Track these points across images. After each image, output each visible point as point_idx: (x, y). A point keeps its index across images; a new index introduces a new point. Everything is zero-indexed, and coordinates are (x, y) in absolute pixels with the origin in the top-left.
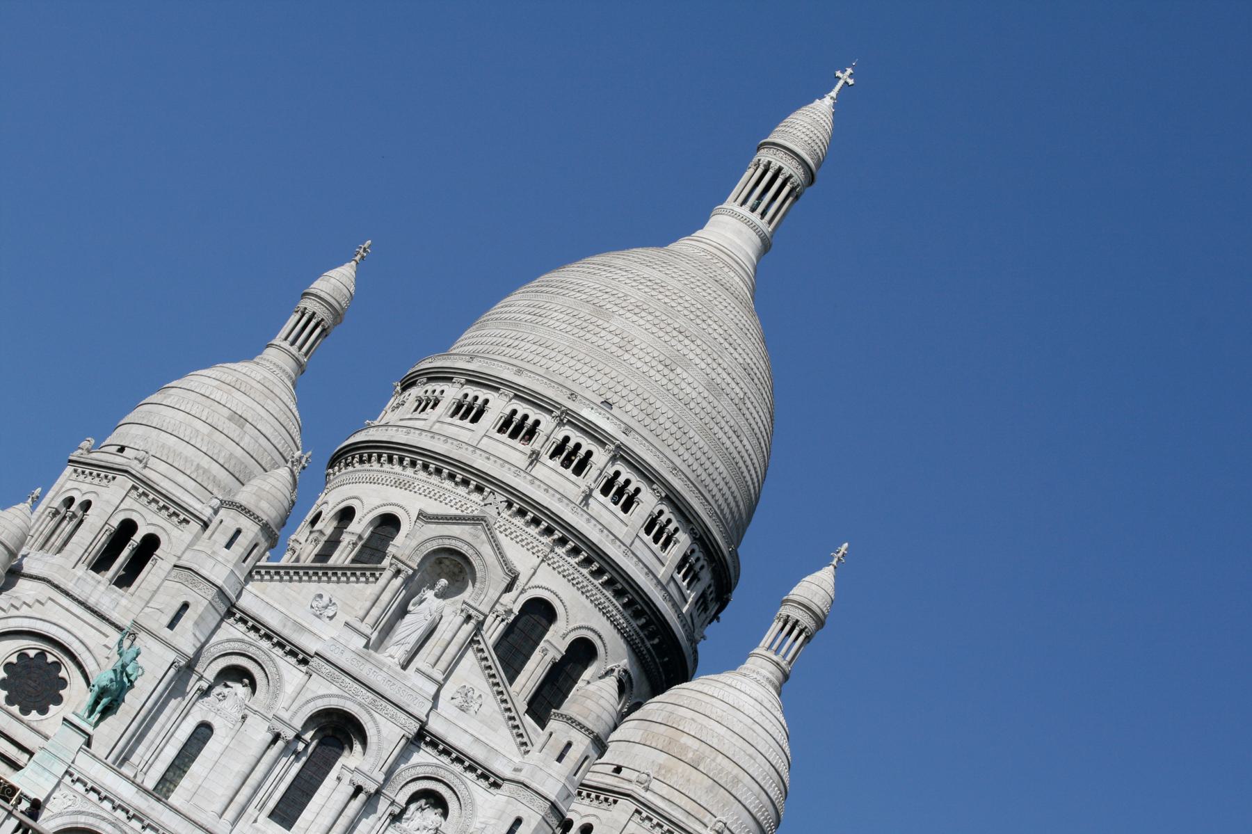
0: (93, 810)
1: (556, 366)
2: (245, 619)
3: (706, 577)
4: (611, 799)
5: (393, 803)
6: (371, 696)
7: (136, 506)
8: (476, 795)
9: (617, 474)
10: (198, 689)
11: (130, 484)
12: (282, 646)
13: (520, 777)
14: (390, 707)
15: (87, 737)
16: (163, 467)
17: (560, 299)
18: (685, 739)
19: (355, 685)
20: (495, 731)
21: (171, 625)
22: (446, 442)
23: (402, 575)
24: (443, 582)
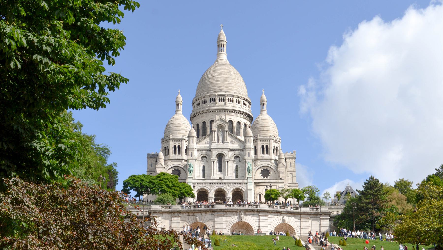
5: (232, 160)
7: (174, 143)
9: (228, 98)
16: (174, 136)
17: (206, 80)
22: (204, 108)
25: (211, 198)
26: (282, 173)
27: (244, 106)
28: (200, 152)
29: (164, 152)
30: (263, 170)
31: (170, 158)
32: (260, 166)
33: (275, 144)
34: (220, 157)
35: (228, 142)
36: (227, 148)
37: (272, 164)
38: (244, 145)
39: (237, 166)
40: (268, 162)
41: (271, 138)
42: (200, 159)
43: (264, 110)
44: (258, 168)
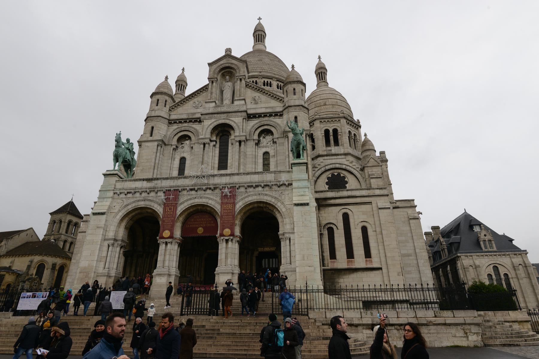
0: (132, 200)
2: (175, 122)
4: (312, 124)
5: (254, 140)
6: (225, 115)
8: (277, 122)
9: (264, 81)
10: (173, 149)
13: (287, 105)
14: (233, 114)
15: (116, 176)
18: (318, 102)
19: (219, 115)
20: (270, 103)
21: (151, 136)
23: (214, 82)
24: (227, 77)
26: (377, 178)
28: (175, 127)
30: (330, 176)
32: (323, 169)
33: (351, 128)
35: (244, 100)
36: (240, 110)
37: (350, 163)
38: (282, 105)
39: (266, 154)
41: (341, 115)
42: (174, 142)
43: (324, 82)
44: (320, 172)
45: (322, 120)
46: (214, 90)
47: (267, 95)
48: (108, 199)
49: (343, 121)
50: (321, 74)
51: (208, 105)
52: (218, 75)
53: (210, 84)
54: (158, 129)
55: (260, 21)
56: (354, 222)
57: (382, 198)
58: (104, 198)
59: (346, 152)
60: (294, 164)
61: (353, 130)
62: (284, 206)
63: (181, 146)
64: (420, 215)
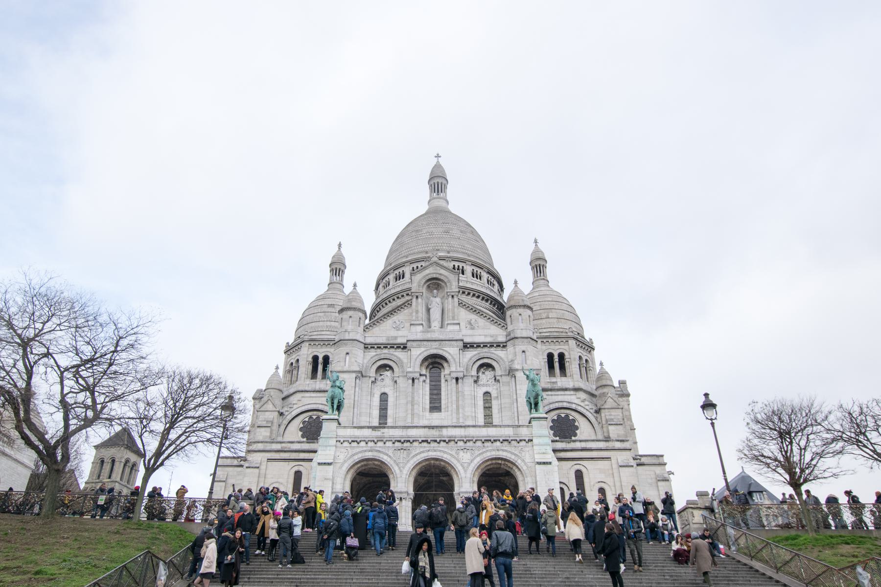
0: (358, 450)
1: (416, 250)
3: (496, 283)
7: (314, 350)
8: (500, 355)
9: (454, 266)
11: (307, 344)
12: (393, 347)
13: (512, 336)
14: (447, 342)
16: (315, 333)
19: (429, 343)
25: (401, 493)
27: (490, 286)
28: (372, 353)
29: (289, 376)
30: (555, 418)
31: (301, 388)
33: (582, 352)
34: (435, 362)
35: (459, 324)
37: (582, 401)
38: (505, 333)
39: (487, 394)
40: (569, 397)
42: (372, 372)
43: (544, 279)
45: (545, 339)
46: (420, 308)
47: (485, 318)
48: (331, 448)
49: (572, 343)
50: (538, 268)
51: (413, 328)
52: (423, 287)
53: (414, 300)
54: (355, 356)
55: (438, 160)
56: (590, 482)
57: (624, 453)
58: (326, 446)
59: (577, 386)
60: (534, 418)
61: (585, 354)
62: (525, 464)
63: (380, 378)
64: (671, 476)
